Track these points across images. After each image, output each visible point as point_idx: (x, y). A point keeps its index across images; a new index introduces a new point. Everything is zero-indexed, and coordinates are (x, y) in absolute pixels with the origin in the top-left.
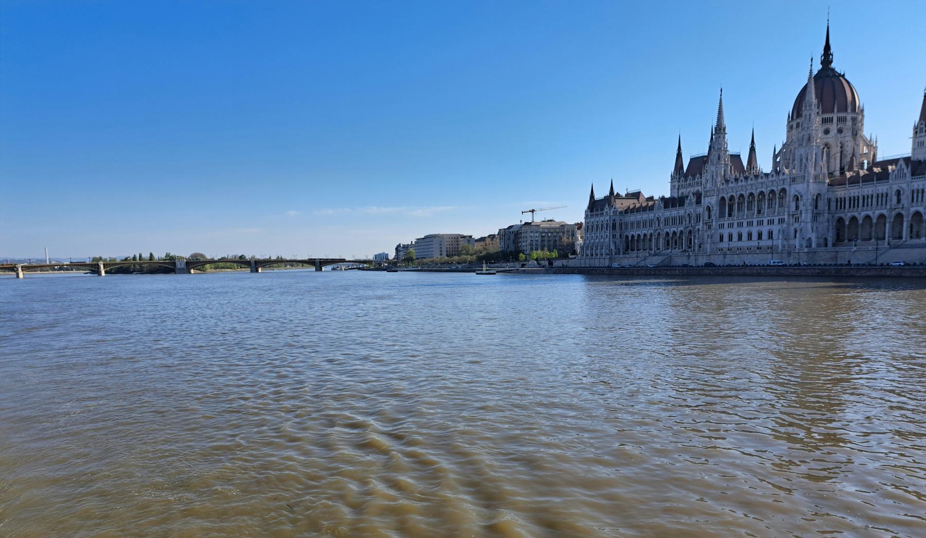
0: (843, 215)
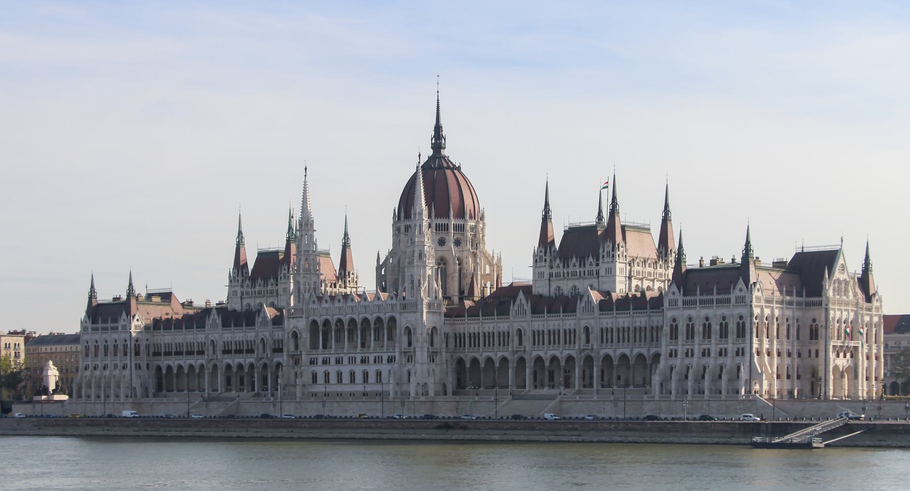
0: (462, 356)
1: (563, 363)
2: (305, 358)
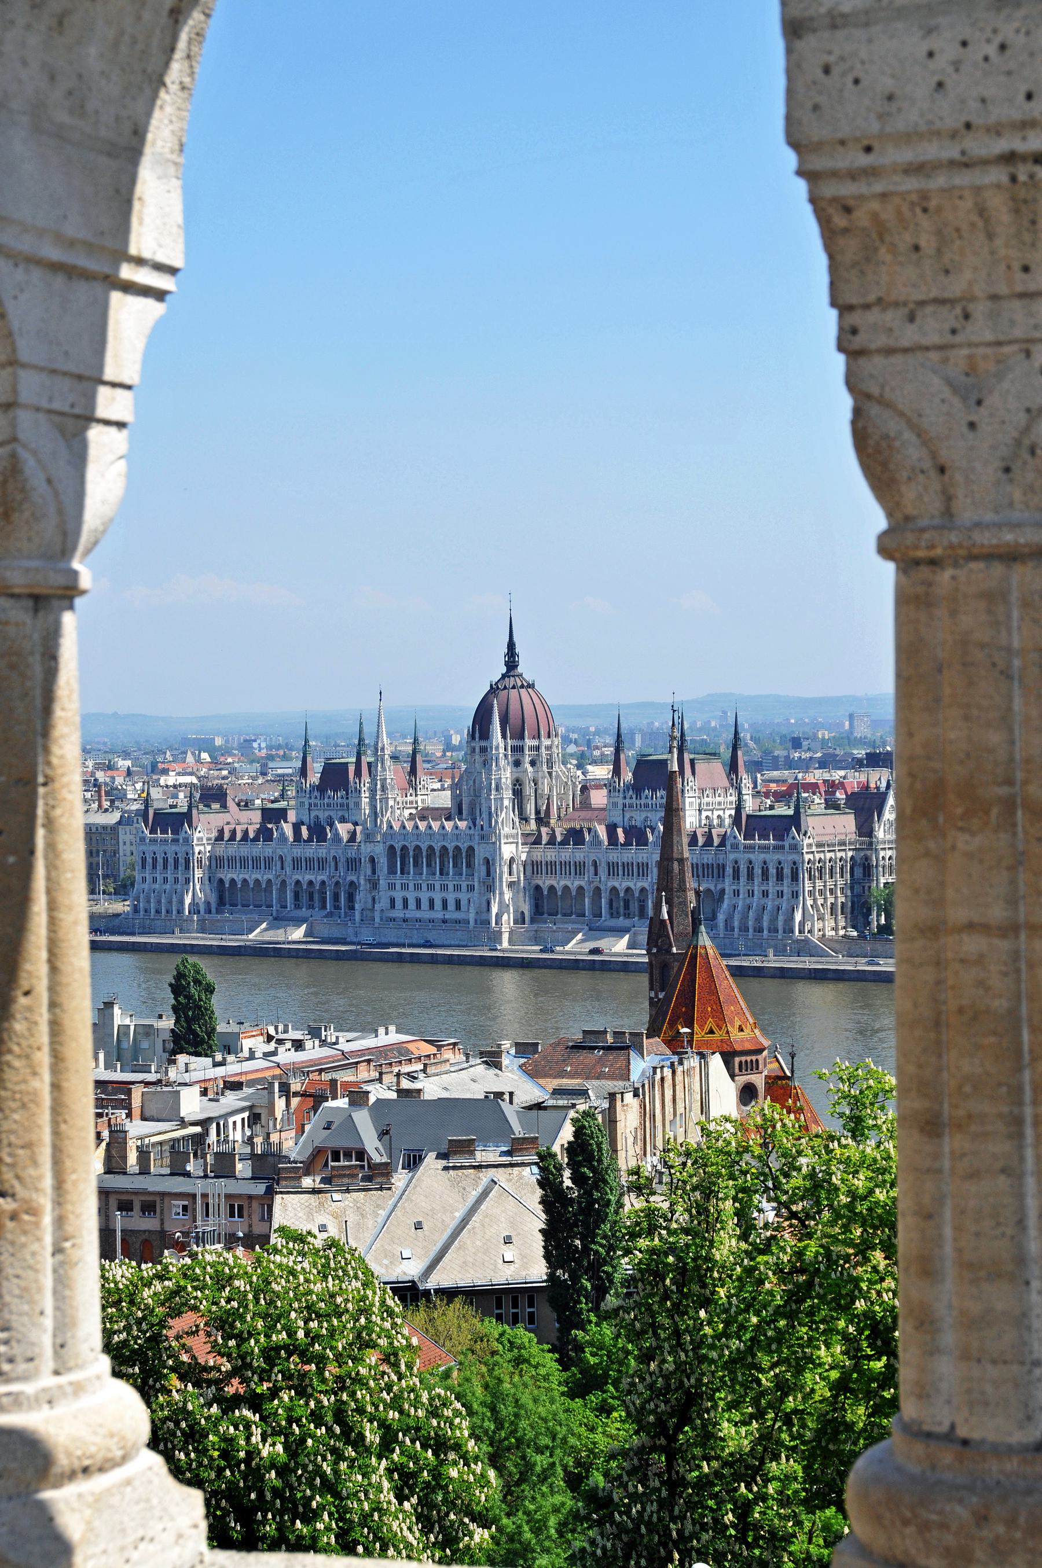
0: (540, 883)
1: (637, 895)
2: (383, 883)
